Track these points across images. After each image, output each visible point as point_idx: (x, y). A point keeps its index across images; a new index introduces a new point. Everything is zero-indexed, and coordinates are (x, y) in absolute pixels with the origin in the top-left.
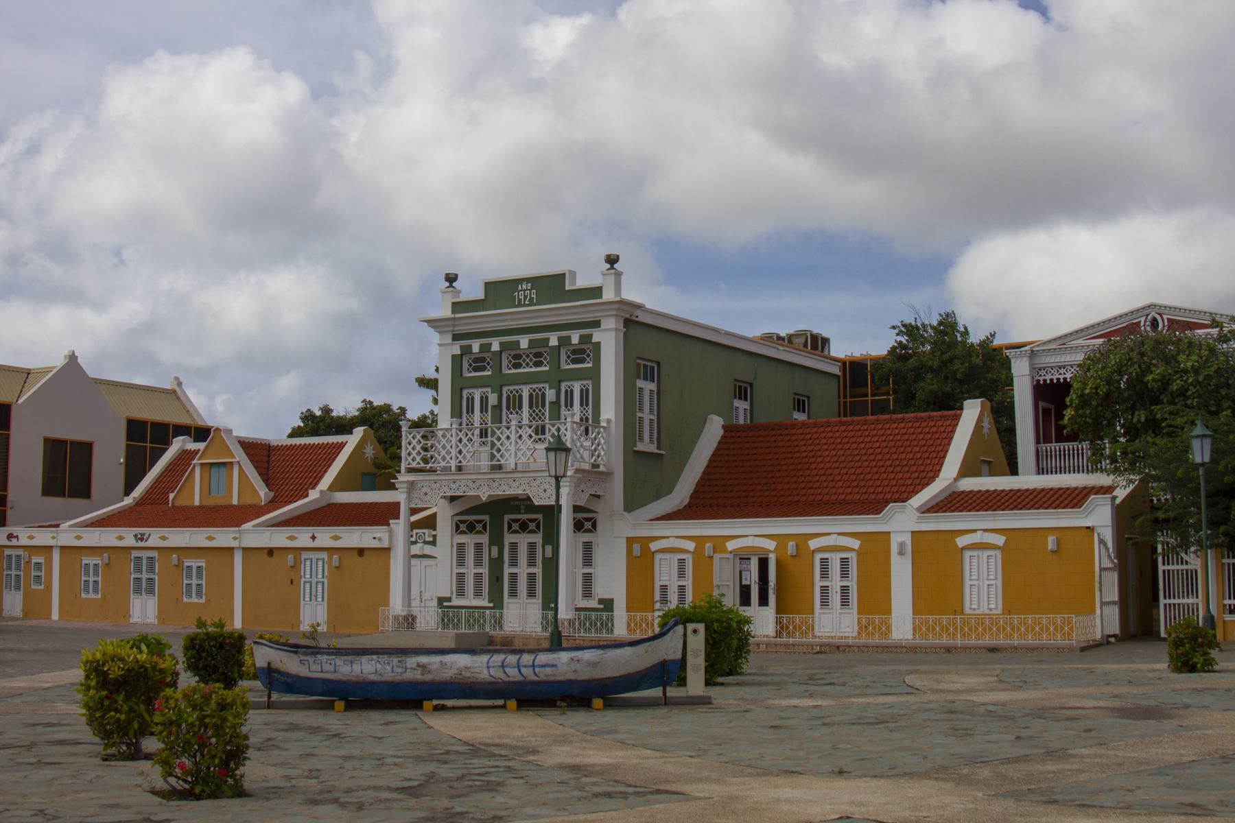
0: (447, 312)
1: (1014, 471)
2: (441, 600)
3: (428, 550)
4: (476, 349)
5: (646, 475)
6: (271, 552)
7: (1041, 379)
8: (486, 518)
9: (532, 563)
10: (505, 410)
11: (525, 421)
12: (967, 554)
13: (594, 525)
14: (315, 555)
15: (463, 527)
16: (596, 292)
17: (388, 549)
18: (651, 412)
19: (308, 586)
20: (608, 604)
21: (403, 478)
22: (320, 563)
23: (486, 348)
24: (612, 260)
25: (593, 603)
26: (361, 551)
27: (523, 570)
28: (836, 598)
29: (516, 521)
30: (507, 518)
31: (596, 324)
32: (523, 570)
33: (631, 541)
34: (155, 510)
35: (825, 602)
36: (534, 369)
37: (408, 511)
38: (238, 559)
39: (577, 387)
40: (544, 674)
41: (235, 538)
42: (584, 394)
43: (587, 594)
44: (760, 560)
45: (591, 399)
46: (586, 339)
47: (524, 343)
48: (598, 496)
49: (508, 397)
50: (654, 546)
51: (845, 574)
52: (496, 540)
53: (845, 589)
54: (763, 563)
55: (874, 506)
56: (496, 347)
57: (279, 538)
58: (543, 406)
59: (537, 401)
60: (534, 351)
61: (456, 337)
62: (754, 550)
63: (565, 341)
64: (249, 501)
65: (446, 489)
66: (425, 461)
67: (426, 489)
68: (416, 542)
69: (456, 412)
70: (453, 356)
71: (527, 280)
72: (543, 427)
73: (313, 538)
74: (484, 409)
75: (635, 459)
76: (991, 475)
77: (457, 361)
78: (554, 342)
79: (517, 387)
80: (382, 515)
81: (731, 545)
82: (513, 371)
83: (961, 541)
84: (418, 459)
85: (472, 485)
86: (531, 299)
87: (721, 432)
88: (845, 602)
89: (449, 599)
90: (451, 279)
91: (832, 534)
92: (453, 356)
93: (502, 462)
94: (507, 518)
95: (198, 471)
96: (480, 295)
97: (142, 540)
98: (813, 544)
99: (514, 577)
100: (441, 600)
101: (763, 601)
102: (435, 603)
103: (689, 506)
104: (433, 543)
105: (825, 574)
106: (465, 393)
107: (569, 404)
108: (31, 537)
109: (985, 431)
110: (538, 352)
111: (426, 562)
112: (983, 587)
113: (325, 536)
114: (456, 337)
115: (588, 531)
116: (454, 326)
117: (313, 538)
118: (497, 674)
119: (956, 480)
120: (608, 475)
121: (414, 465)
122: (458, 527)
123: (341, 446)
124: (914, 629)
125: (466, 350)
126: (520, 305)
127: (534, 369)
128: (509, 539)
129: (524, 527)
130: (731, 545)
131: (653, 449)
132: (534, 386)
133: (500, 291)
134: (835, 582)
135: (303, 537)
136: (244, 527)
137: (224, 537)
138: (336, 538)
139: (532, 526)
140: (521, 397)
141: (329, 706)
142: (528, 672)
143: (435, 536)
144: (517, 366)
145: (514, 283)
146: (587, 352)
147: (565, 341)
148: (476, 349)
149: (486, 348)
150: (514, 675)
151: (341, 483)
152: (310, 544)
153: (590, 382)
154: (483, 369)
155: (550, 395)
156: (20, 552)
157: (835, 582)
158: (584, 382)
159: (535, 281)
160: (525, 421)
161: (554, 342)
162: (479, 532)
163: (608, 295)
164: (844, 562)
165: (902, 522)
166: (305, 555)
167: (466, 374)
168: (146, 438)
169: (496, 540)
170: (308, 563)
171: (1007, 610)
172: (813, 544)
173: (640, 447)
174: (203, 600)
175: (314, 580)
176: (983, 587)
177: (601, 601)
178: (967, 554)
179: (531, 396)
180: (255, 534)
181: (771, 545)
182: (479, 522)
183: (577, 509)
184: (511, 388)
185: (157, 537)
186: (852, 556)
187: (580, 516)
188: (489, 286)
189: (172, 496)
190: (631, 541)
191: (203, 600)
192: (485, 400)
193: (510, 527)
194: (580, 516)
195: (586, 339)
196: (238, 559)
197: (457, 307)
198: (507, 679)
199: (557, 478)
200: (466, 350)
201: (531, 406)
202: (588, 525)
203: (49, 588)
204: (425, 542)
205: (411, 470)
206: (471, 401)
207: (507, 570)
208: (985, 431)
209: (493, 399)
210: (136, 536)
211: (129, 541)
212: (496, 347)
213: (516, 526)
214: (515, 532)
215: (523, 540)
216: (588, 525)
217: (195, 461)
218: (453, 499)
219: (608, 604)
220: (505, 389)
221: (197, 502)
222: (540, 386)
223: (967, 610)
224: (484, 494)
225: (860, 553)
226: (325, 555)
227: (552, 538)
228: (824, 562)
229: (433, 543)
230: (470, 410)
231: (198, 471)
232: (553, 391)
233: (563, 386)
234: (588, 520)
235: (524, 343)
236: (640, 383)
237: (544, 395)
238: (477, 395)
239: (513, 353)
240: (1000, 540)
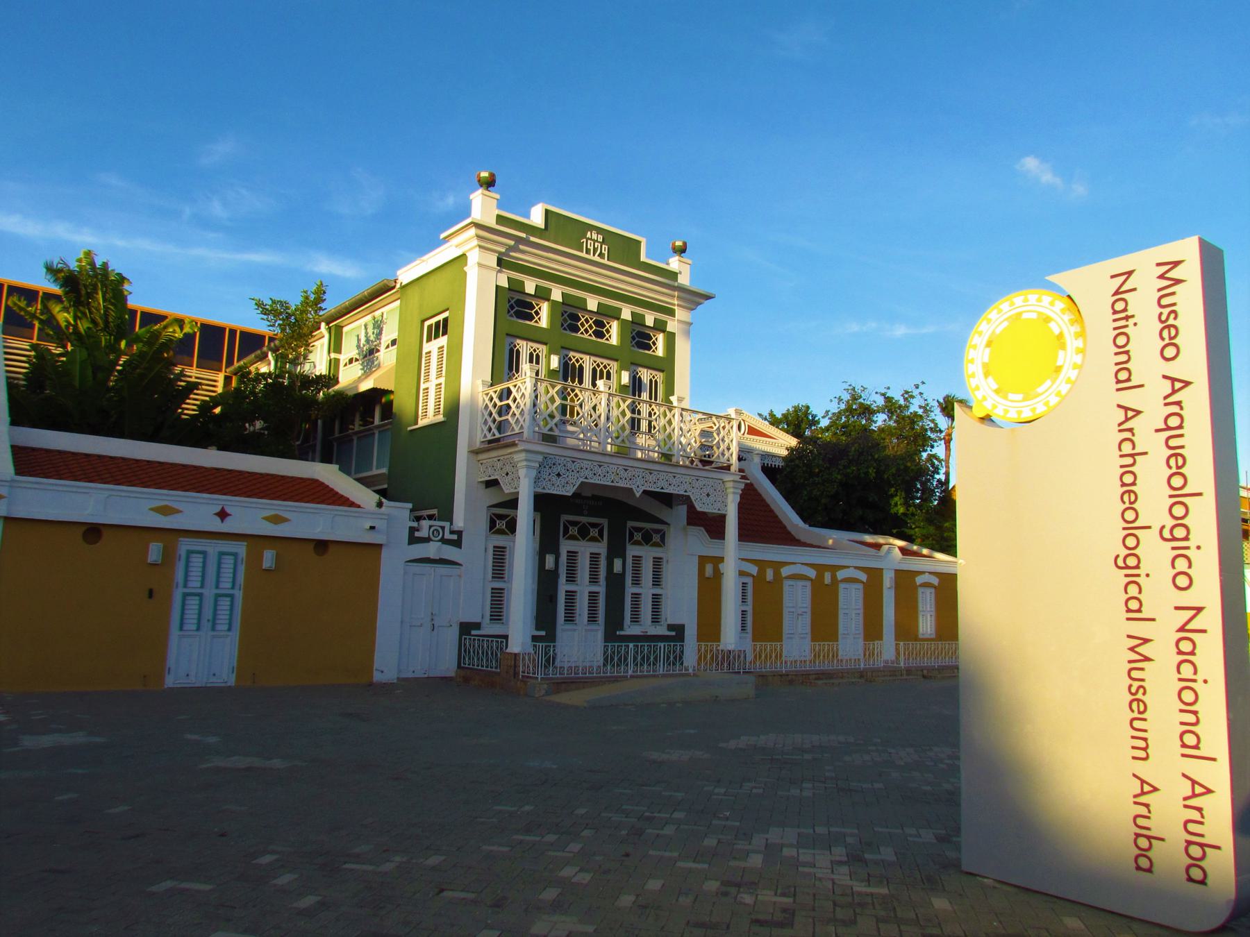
2: (466, 628)
3: (450, 553)
6: (93, 532)
9: (594, 579)
14: (213, 547)
15: (501, 524)
17: (381, 545)
20: (678, 631)
22: (228, 562)
23: (542, 294)
25: (661, 630)
26: (321, 546)
27: (583, 588)
29: (574, 523)
30: (565, 518)
32: (583, 588)
33: (703, 560)
43: (656, 619)
46: (660, 327)
47: (592, 303)
63: (638, 320)
68: (428, 540)
71: (599, 231)
85: (622, 473)
89: (477, 626)
99: (571, 595)
102: (456, 630)
104: (457, 543)
111: (443, 570)
115: (656, 545)
117: (223, 515)
128: (566, 546)
129: (584, 533)
132: (599, 360)
139: (594, 532)
149: (542, 294)
152: (216, 525)
161: (626, 314)
166: (185, 545)
175: (209, 592)
177: (670, 627)
179: (594, 370)
190: (703, 560)
193: (566, 530)
202: (656, 538)
204: (445, 541)
207: (563, 587)
214: (573, 538)
215: (585, 549)
219: (678, 631)
226: (241, 549)
229: (457, 543)
234: (657, 531)
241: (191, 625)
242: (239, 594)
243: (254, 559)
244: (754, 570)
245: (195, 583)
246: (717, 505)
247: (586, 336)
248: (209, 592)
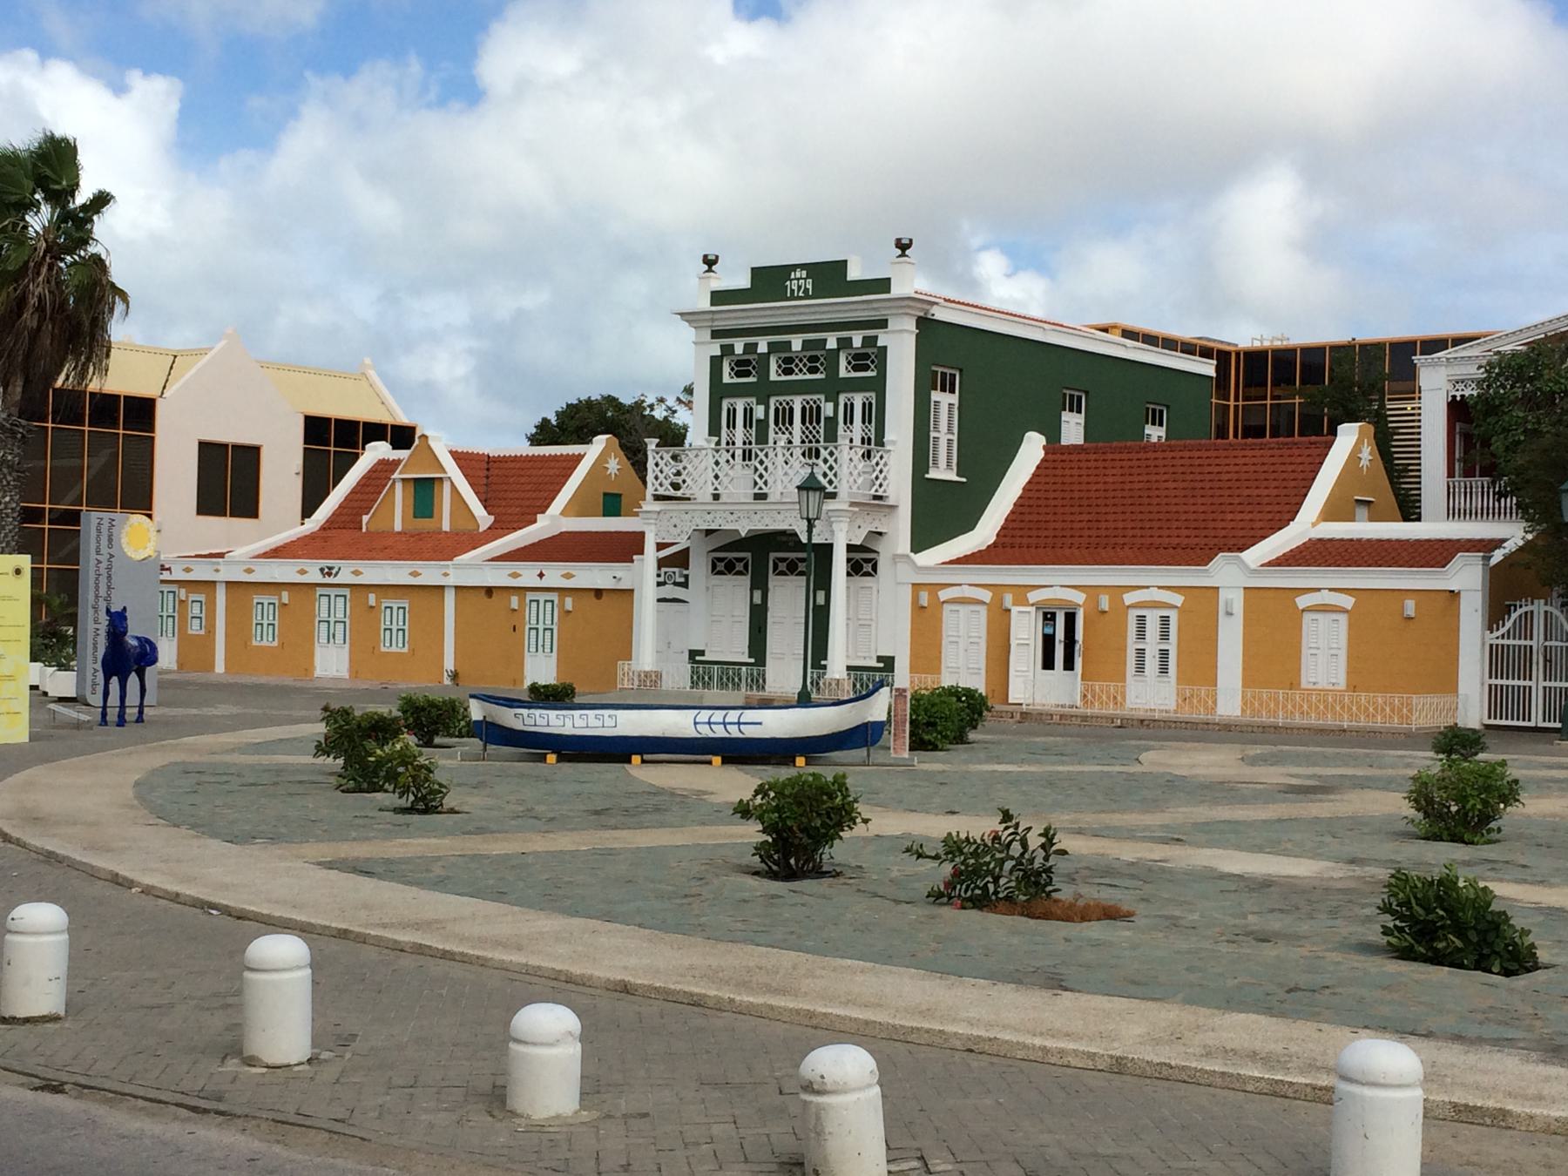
0: (704, 304)
1: (1409, 509)
3: (679, 593)
4: (739, 349)
5: (940, 511)
6: (489, 591)
7: (1458, 394)
8: (748, 555)
10: (772, 425)
11: (797, 441)
12: (1307, 617)
13: (875, 568)
14: (542, 597)
15: (721, 566)
16: (883, 285)
18: (950, 431)
19: (533, 633)
21: (649, 505)
22: (549, 605)
24: (903, 247)
26: (598, 593)
28: (1152, 663)
29: (783, 560)
30: (773, 556)
31: (883, 324)
34: (346, 535)
35: (1140, 667)
36: (809, 376)
37: (654, 547)
38: (450, 598)
39: (858, 400)
40: (750, 732)
41: (446, 575)
42: (867, 407)
44: (1067, 615)
45: (876, 415)
46: (870, 341)
47: (797, 343)
48: (880, 534)
49: (777, 410)
50: (944, 595)
51: (1165, 636)
52: (759, 583)
53: (1164, 654)
54: (1070, 619)
55: (1201, 556)
56: (763, 348)
57: (498, 576)
58: (818, 422)
59: (811, 415)
60: (809, 354)
61: (716, 334)
62: (1062, 604)
63: (845, 343)
64: (465, 525)
65: (699, 521)
66: (676, 486)
67: (674, 521)
69: (714, 430)
70: (712, 358)
71: (802, 266)
72: (818, 451)
73: (541, 575)
74: (748, 421)
75: (924, 488)
76: (1371, 519)
77: (716, 363)
78: (832, 344)
79: (788, 398)
80: (626, 548)
81: (1034, 597)
82: (784, 378)
83: (1303, 602)
84: (667, 483)
86: (806, 290)
87: (1042, 454)
88: (1164, 669)
89: (702, 653)
90: (710, 262)
91: (1152, 586)
92: (712, 358)
93: (765, 490)
94: (773, 556)
95: (399, 486)
96: (744, 282)
97: (329, 574)
98: (1129, 598)
100: (693, 654)
101: (1069, 665)
103: (995, 545)
104: (685, 585)
105: (1141, 633)
106: (725, 404)
107: (849, 419)
108: (188, 570)
109: (1364, 463)
110: (816, 356)
112: (1325, 656)
113: (555, 574)
114: (716, 334)
116: (713, 320)
118: (705, 731)
119: (1314, 525)
120: (893, 507)
121: (661, 491)
122: (714, 567)
123: (578, 458)
124: (1245, 703)
125: (727, 350)
126: (793, 298)
127: (809, 376)
129: (792, 568)
130: (1034, 597)
131: (952, 476)
132: (808, 397)
133: (769, 281)
134: (1152, 645)
135: (528, 574)
136: (458, 560)
137: (430, 573)
138: (568, 576)
140: (791, 410)
141: (543, 758)
142: (734, 732)
143: (687, 577)
144: (788, 372)
145: (785, 271)
146: (872, 359)
147: (845, 343)
148: (739, 349)
150: (720, 732)
151: (578, 507)
153: (873, 395)
154: (748, 374)
155: (828, 409)
156: (174, 588)
157: (1152, 645)
158: (867, 395)
159: (813, 269)
160: (797, 441)
161: (832, 344)
162: (739, 573)
163: (897, 290)
164: (1165, 621)
165: (1232, 575)
166: (530, 596)
167: (726, 379)
168: (331, 442)
169: (759, 583)
170: (534, 605)
171: (1353, 687)
172: (1129, 598)
173: (933, 474)
174: (405, 650)
176: (1325, 656)
177: (880, 659)
178: (1307, 617)
179: (804, 409)
180: (473, 568)
181: (1079, 598)
182: (740, 560)
183: (851, 548)
184: (781, 399)
185: (347, 572)
186: (1174, 616)
187: (858, 556)
188: (757, 273)
189: (365, 518)
191: (405, 650)
192: (748, 412)
193: (776, 567)
194: (858, 556)
195: (870, 341)
196: (450, 598)
197: (718, 297)
198: (711, 735)
199: (809, 520)
200: (727, 350)
201: (803, 422)
202: (868, 568)
203: (211, 631)
204: (676, 584)
205: (658, 498)
206: (732, 413)
208: (1364, 463)
209: (759, 412)
210: (322, 570)
211: (314, 576)
212: (763, 348)
213: (782, 567)
214: (782, 573)
216: (868, 568)
217: (396, 475)
218: (709, 532)
220: (772, 401)
221: (398, 527)
222: (815, 397)
223: (1304, 685)
224: (743, 529)
225: (1182, 610)
226: (554, 597)
227: (823, 581)
228: (1141, 619)
229: (685, 585)
230: (732, 424)
231: (399, 486)
232: (830, 406)
233: (842, 399)
234: (868, 561)
235: (797, 343)
236: (936, 396)
237: (819, 408)
238: (740, 405)
239: (784, 355)
240: (1348, 602)
241: (533, 649)
242: (555, 628)
243: (562, 603)
244: (986, 596)
245: (534, 621)
246: (827, 535)
247: (800, 377)
248: (541, 627)
